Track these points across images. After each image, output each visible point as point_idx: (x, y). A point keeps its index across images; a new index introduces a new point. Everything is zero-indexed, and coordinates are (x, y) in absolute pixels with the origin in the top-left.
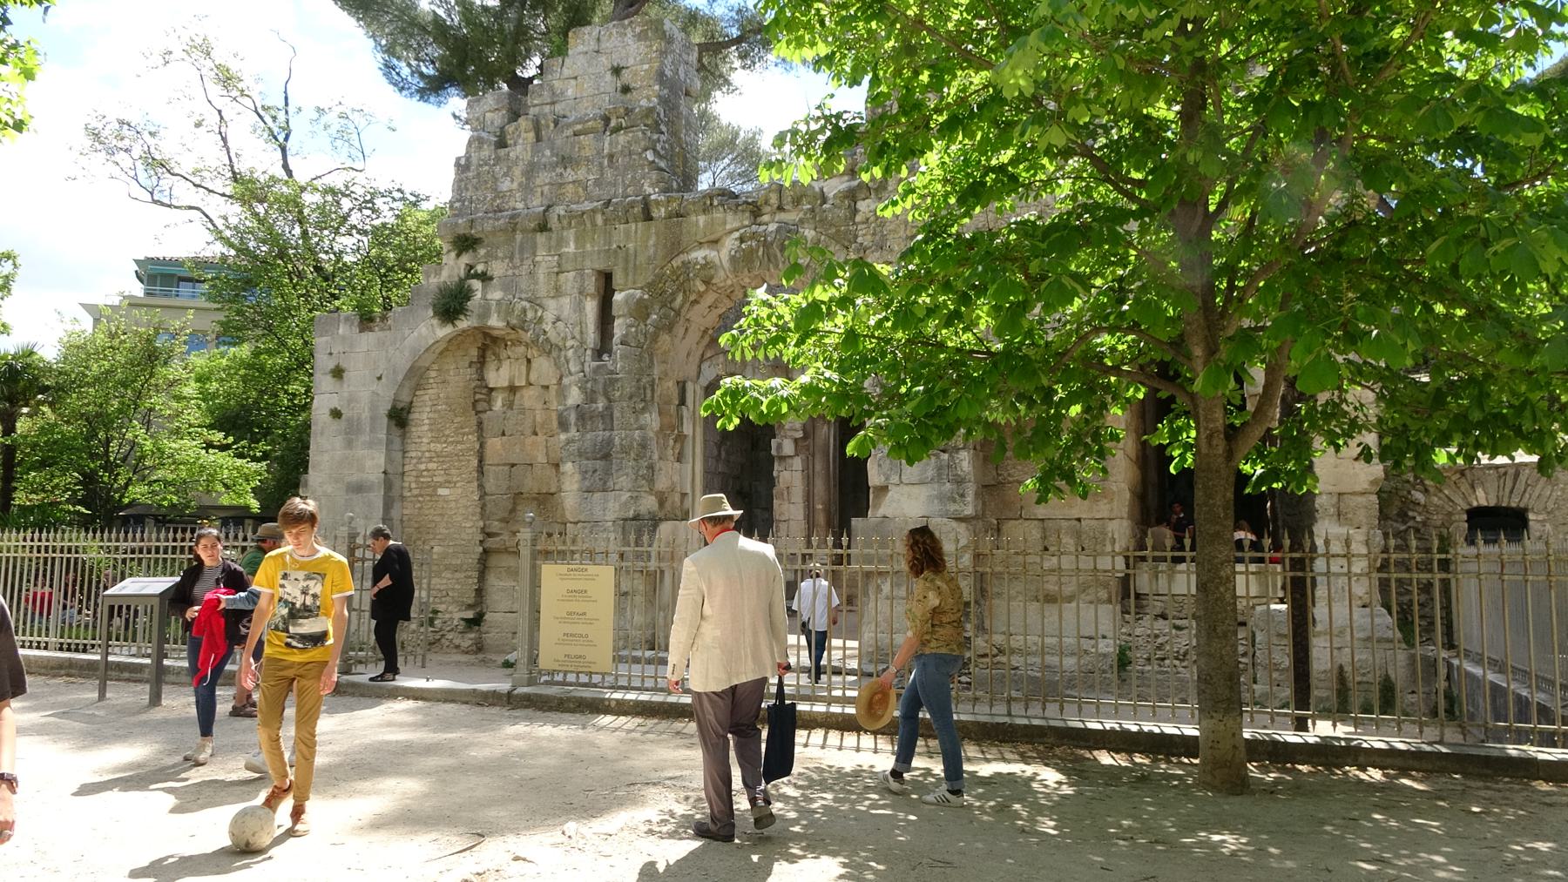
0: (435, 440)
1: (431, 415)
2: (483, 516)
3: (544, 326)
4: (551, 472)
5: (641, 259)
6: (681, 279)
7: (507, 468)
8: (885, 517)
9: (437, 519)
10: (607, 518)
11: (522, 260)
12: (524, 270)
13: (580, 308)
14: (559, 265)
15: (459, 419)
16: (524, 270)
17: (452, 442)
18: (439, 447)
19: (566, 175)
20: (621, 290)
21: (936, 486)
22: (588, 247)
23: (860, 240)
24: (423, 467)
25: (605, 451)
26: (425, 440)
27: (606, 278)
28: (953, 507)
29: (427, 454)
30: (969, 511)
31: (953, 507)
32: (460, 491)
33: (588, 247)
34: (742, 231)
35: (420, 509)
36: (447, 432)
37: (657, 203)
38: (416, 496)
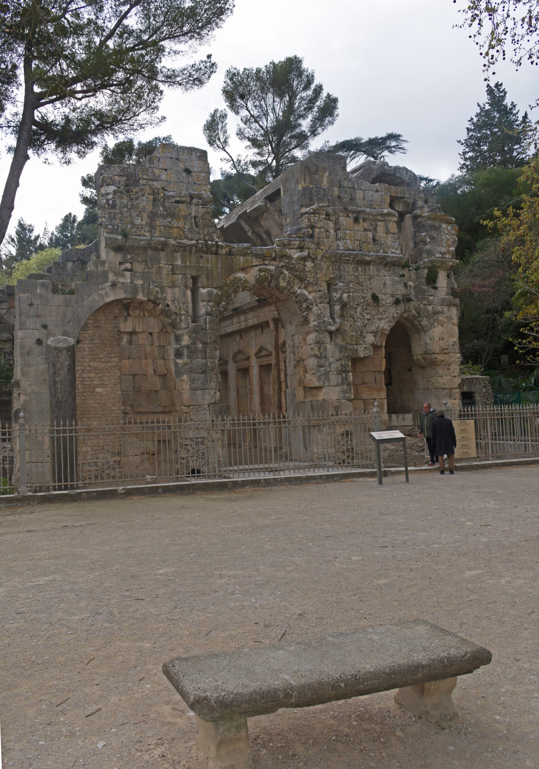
0: (94, 360)
1: (90, 346)
2: (124, 404)
3: (167, 302)
4: (157, 379)
5: (215, 273)
6: (235, 286)
7: (131, 377)
8: (324, 400)
9: (95, 405)
10: (205, 403)
11: (152, 265)
12: (154, 270)
13: (185, 295)
14: (172, 270)
15: (108, 349)
16: (154, 270)
17: (104, 362)
18: (96, 364)
19: (173, 223)
20: (204, 288)
21: (342, 387)
22: (188, 263)
23: (308, 279)
24: (85, 375)
25: (204, 369)
26: (86, 360)
27: (195, 279)
28: (348, 395)
29: (88, 368)
30: (353, 397)
31: (348, 395)
32: (110, 390)
33: (188, 263)
34: (260, 267)
35: (84, 400)
36: (101, 356)
37: (222, 247)
38: (83, 392)
